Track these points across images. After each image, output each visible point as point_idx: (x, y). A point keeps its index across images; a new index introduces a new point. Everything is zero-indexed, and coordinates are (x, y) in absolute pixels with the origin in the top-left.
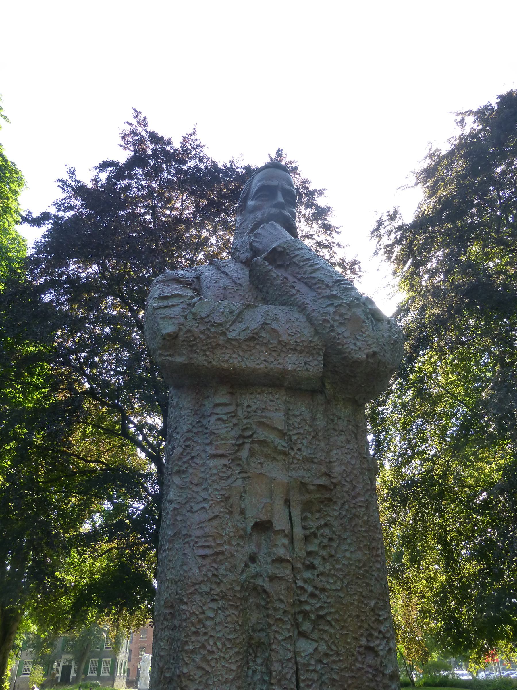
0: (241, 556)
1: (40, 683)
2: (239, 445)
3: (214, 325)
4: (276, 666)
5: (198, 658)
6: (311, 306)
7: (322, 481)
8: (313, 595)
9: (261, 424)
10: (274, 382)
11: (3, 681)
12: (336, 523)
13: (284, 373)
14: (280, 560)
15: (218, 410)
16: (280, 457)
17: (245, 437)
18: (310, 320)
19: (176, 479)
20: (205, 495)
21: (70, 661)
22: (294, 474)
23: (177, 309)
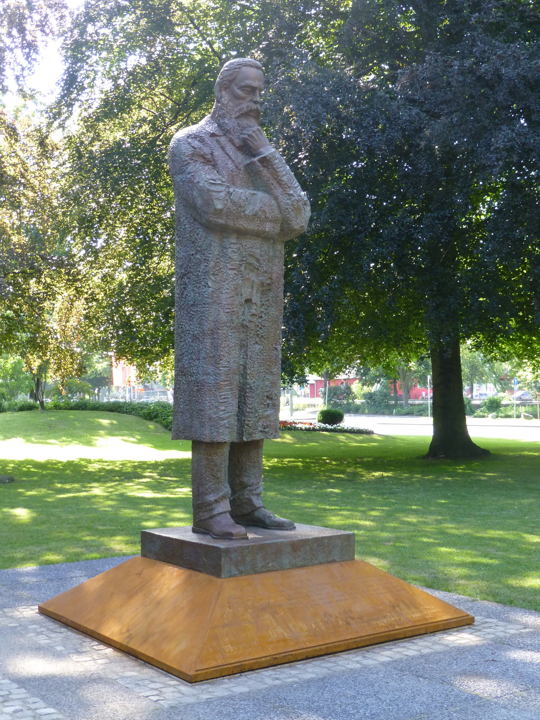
2: (241, 265)
3: (240, 207)
4: (249, 353)
5: (226, 349)
6: (281, 198)
7: (269, 282)
8: (261, 328)
9: (250, 255)
12: (271, 299)
13: (265, 232)
14: (253, 315)
15: (232, 246)
16: (255, 270)
17: (243, 261)
18: (279, 206)
19: (213, 278)
20: (227, 286)
22: (259, 278)
23: (222, 194)
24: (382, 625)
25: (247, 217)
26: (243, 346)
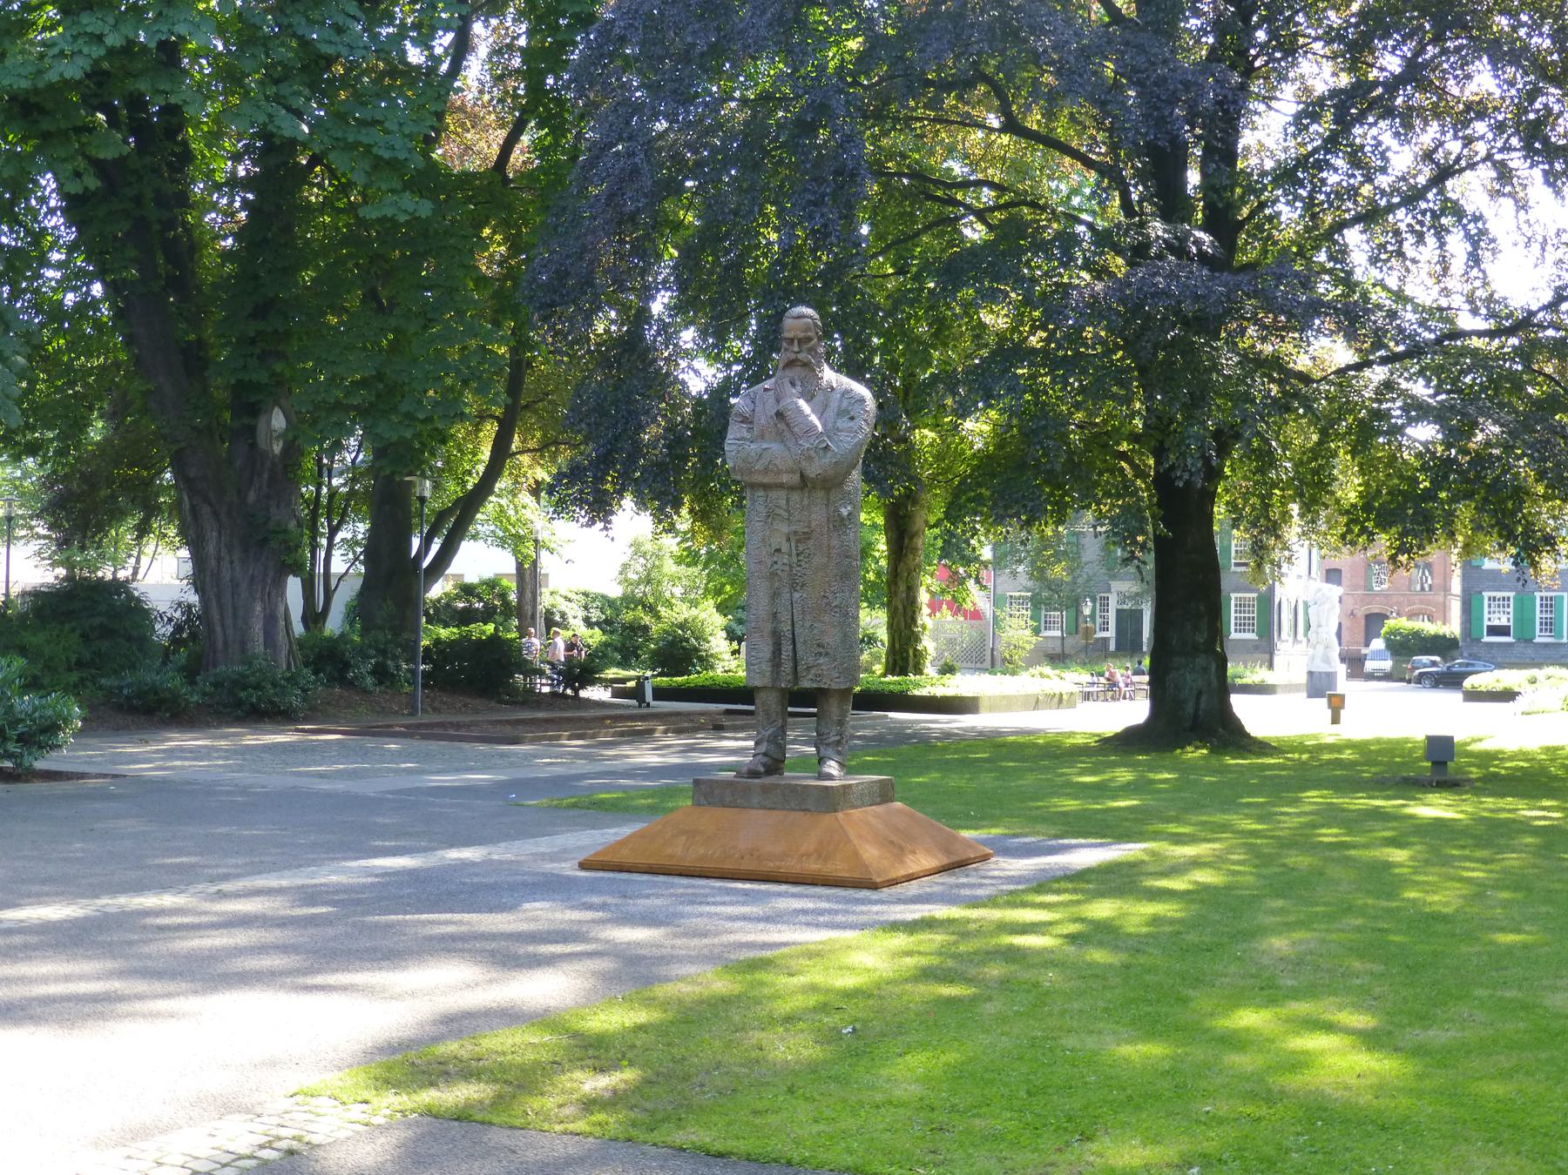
0: (769, 563)
10: (781, 486)
11: (918, 639)
24: (769, 866)
25: (759, 472)
26: (775, 595)
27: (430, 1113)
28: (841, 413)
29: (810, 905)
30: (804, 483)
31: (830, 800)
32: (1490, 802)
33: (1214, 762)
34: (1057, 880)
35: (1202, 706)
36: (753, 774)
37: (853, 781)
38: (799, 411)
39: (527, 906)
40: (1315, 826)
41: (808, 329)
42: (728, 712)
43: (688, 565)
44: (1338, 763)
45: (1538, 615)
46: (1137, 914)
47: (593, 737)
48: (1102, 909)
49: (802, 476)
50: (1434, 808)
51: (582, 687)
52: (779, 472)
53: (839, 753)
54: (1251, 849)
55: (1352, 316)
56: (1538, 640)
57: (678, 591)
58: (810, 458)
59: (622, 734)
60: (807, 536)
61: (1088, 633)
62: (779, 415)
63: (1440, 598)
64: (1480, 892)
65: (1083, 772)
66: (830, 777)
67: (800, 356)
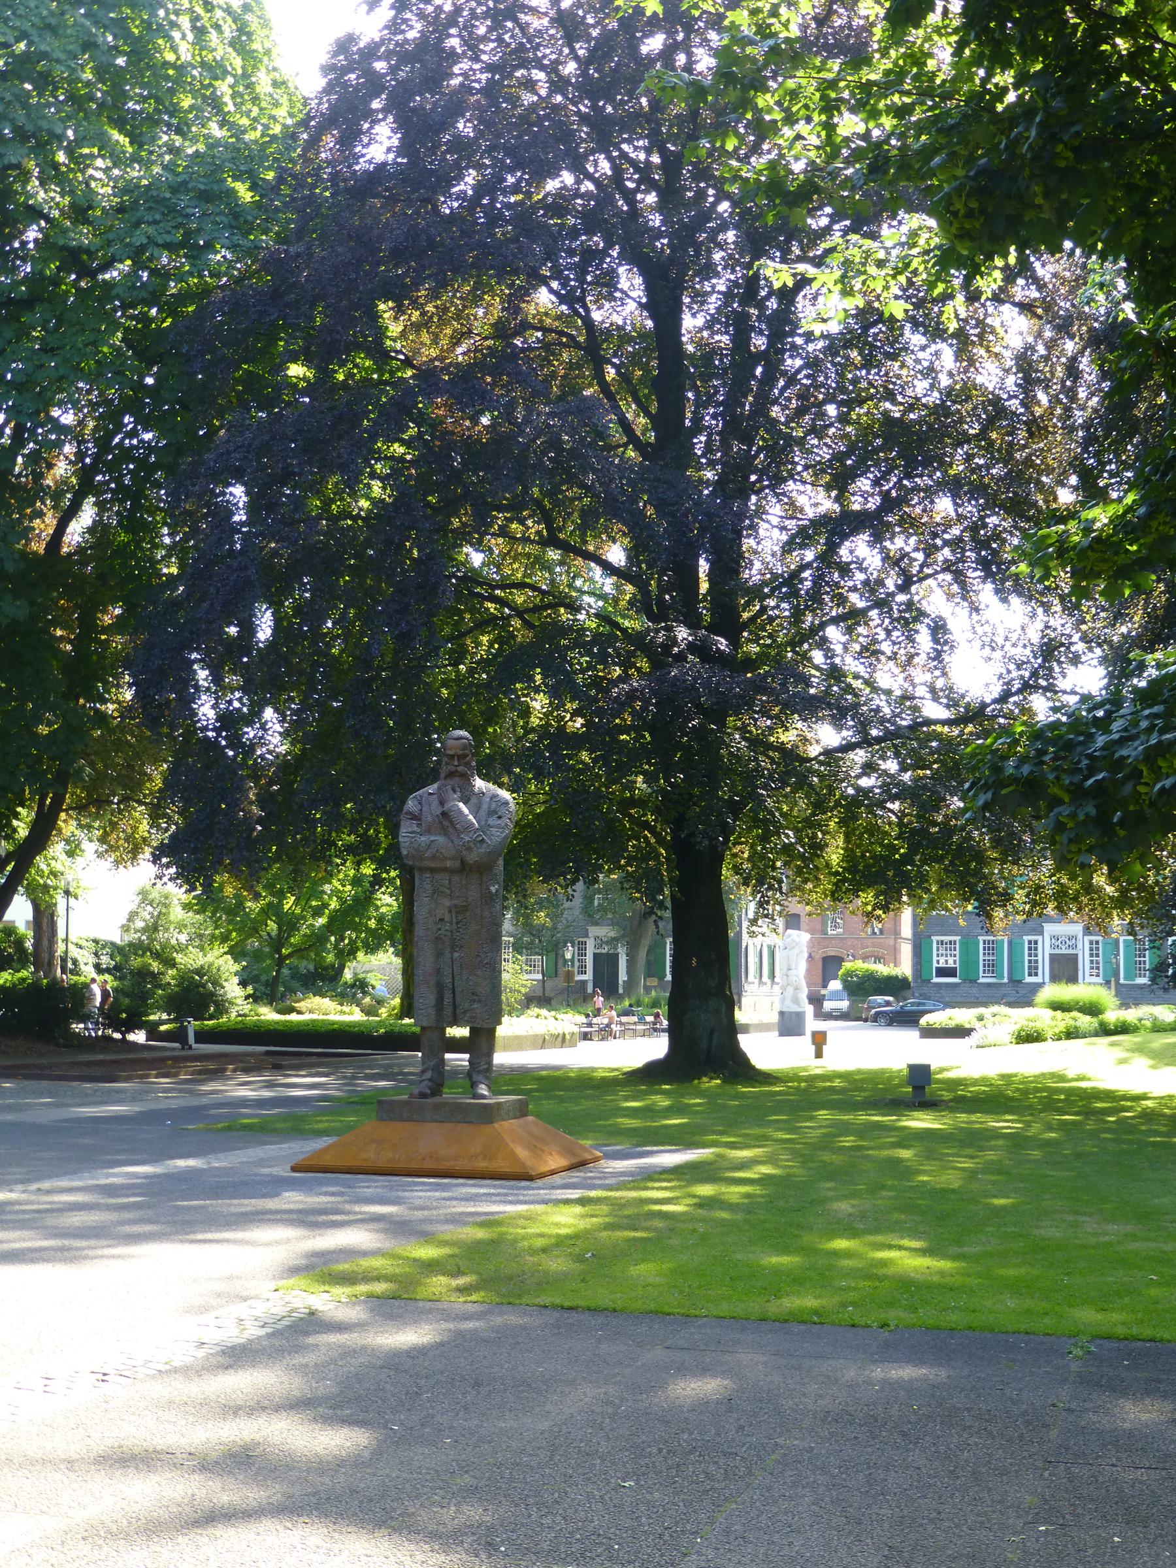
1: (523, 990)
10: (445, 870)
21: (612, 942)
24: (446, 1165)
26: (439, 955)
27: (370, 1296)
28: (491, 813)
29: (482, 1191)
30: (464, 868)
31: (488, 1114)
32: (963, 1116)
33: (728, 1088)
34: (661, 1173)
35: (715, 1042)
36: (423, 1095)
37: (502, 1099)
38: (460, 812)
39: (287, 1194)
40: (835, 1136)
41: (464, 747)
42: (268, 1053)
43: (198, 912)
44: (832, 1090)
45: (981, 957)
46: (734, 1193)
47: (176, 1075)
48: (706, 1190)
49: (462, 862)
50: (921, 1121)
51: (130, 1030)
52: (445, 859)
53: (487, 1078)
54: (795, 1153)
55: (837, 704)
56: (981, 980)
57: (183, 938)
58: (469, 849)
59: (200, 1073)
60: (465, 908)
61: (569, 976)
62: (445, 815)
63: (891, 942)
64: (972, 1175)
65: (627, 1099)
66: (483, 1097)
67: (460, 769)
